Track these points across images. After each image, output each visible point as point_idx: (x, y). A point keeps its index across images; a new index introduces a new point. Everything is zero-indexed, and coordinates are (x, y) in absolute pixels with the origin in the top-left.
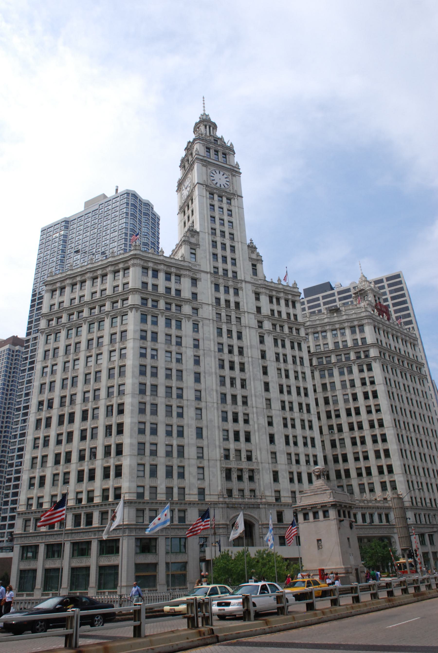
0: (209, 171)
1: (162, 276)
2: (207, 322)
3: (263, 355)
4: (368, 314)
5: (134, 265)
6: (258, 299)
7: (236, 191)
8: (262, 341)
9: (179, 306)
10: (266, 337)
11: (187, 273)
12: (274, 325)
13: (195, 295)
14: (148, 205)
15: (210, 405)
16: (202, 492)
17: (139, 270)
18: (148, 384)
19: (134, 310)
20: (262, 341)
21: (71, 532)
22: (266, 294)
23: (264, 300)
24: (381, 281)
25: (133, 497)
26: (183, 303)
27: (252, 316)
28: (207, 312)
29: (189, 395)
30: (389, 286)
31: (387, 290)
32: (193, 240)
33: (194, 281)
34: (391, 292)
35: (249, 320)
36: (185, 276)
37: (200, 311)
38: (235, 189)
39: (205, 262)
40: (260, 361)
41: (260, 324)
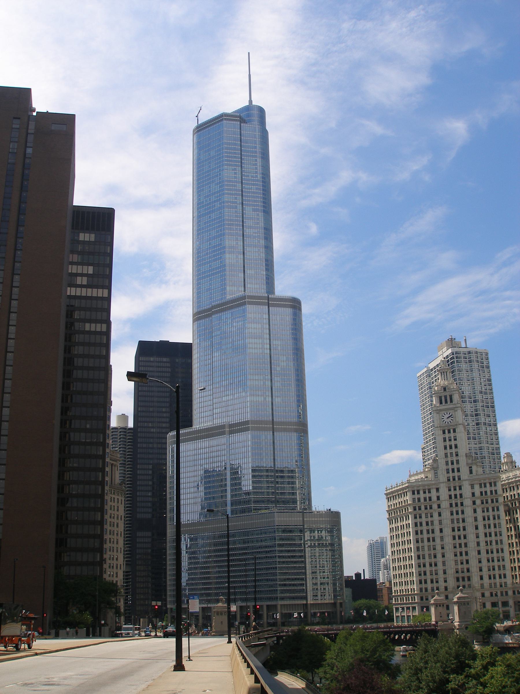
0: (441, 415)
1: (421, 492)
3: (476, 519)
7: (458, 422)
8: (475, 511)
11: (434, 486)
16: (446, 588)
20: (475, 511)
22: (477, 483)
23: (477, 487)
25: (419, 592)
27: (469, 500)
28: (445, 504)
29: (438, 548)
33: (438, 490)
35: (468, 502)
36: (432, 488)
37: (441, 506)
38: (457, 420)
39: (443, 477)
40: (474, 523)
41: (474, 503)
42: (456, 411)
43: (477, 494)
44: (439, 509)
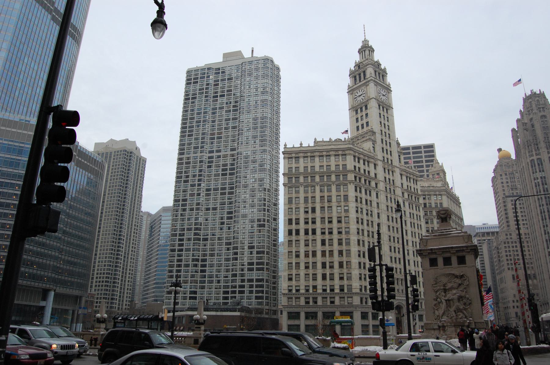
1: (361, 161)
2: (382, 192)
4: (444, 188)
5: (350, 154)
6: (402, 179)
9: (369, 182)
10: (405, 202)
12: (408, 195)
13: (375, 174)
14: (278, 69)
15: (385, 242)
17: (352, 157)
18: (360, 229)
19: (352, 184)
21: (322, 307)
24: (419, 147)
26: (372, 180)
27: (400, 189)
28: (381, 186)
30: (425, 152)
31: (423, 154)
32: (372, 138)
34: (426, 157)
37: (378, 185)
42: (389, 93)
43: (405, 187)
44: (377, 190)
